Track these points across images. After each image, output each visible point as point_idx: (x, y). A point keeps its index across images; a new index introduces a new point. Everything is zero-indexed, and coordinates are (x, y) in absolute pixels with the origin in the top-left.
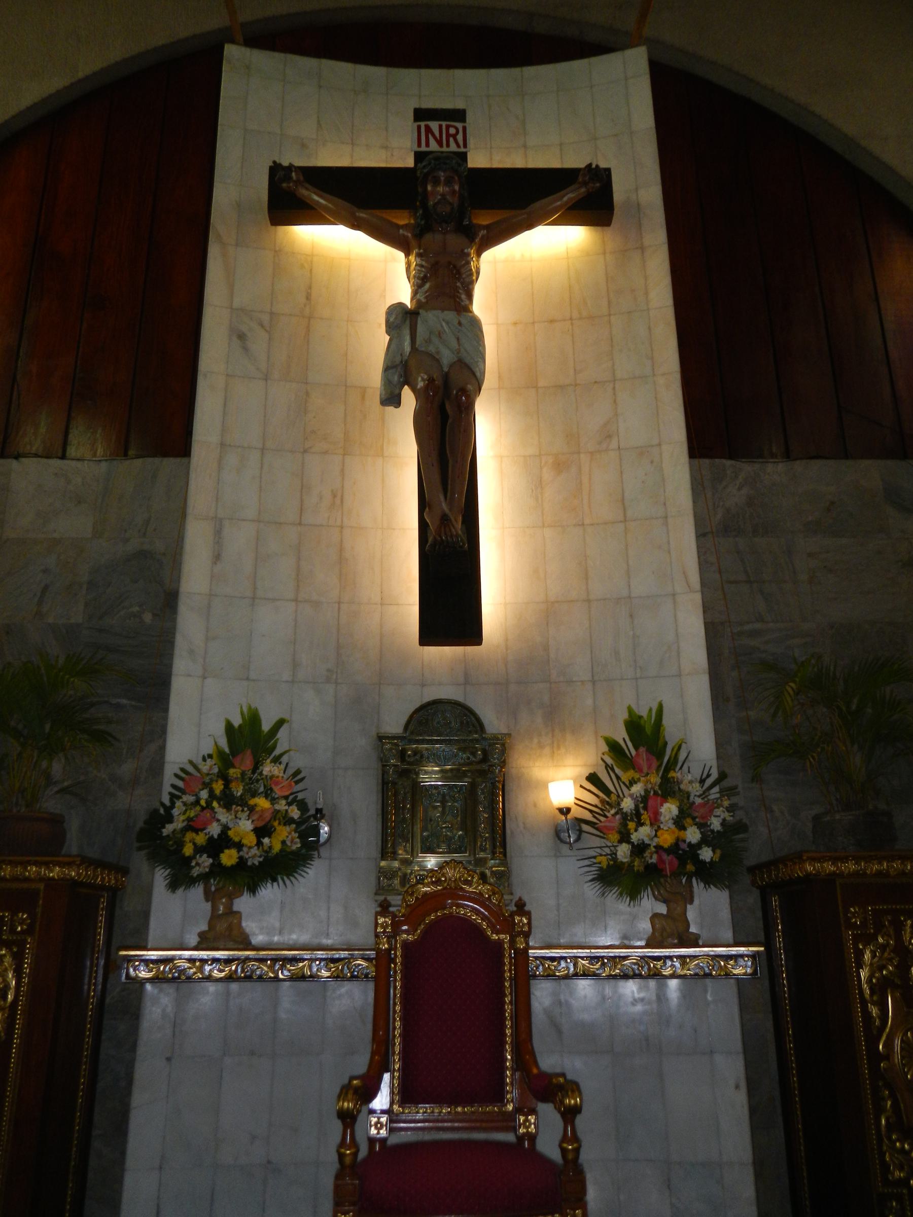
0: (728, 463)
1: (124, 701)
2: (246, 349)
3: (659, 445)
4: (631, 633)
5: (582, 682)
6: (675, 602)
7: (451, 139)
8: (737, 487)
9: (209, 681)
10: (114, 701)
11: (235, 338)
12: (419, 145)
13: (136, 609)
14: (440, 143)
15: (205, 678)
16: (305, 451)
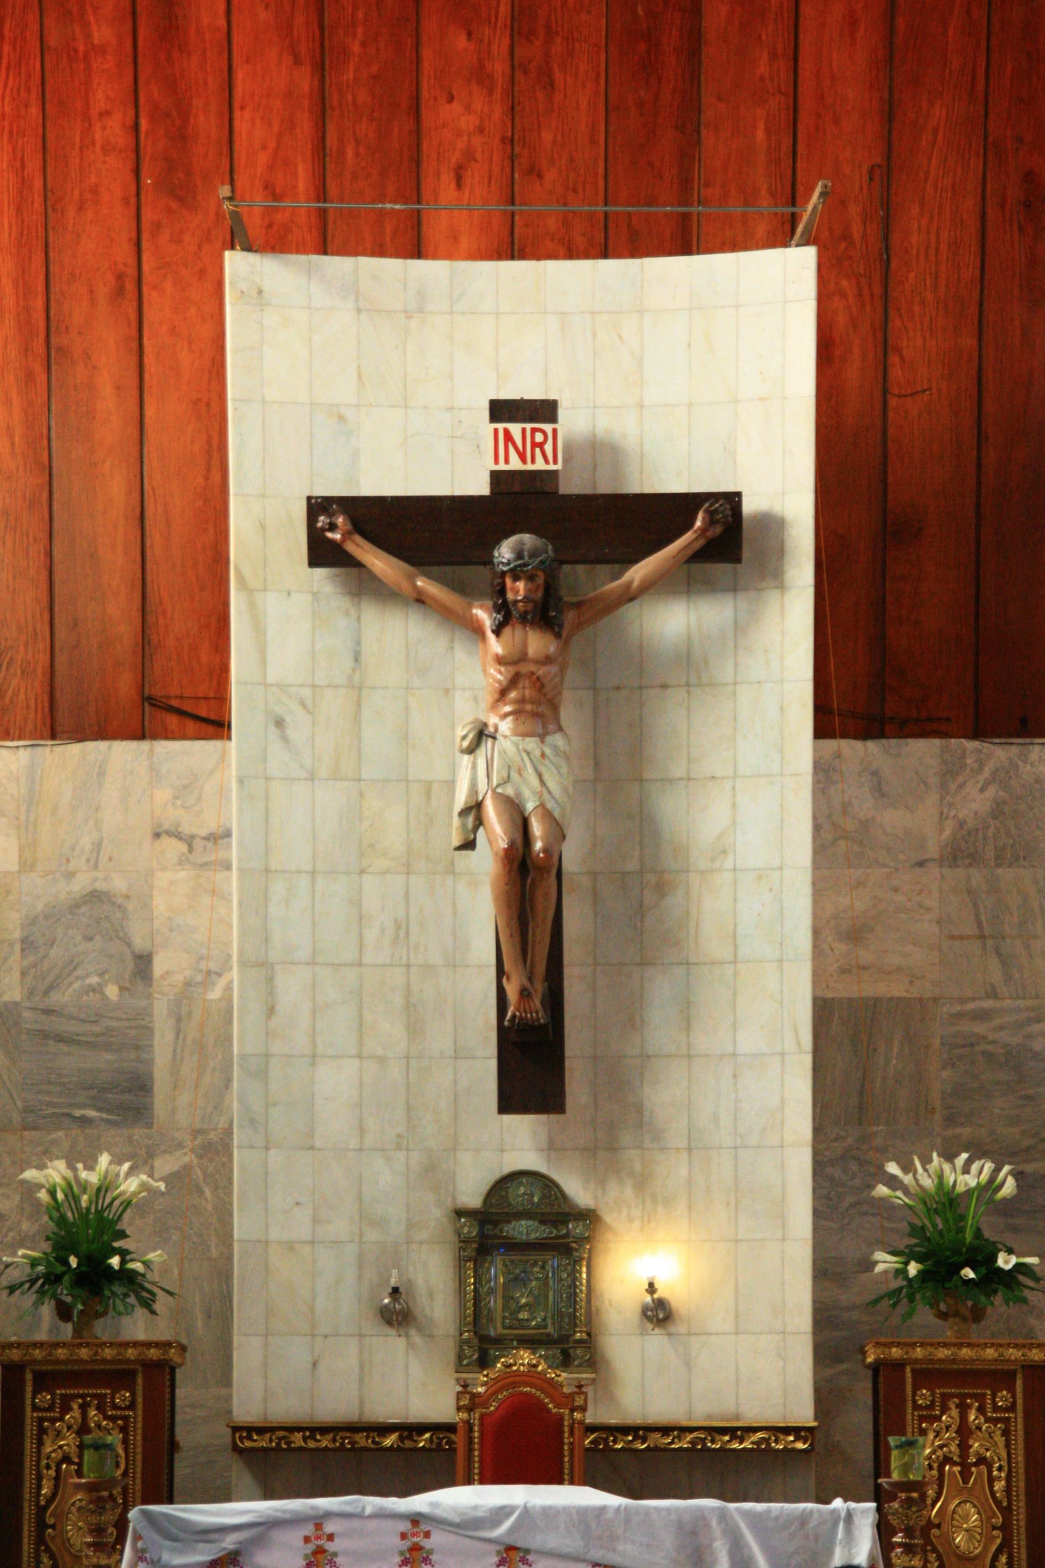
0: (971, 745)
1: (92, 1113)
2: (285, 739)
3: (781, 868)
4: (734, 1095)
5: (678, 1149)
6: (783, 1061)
7: (538, 450)
8: (979, 786)
9: (272, 1152)
10: (78, 1113)
11: (272, 728)
12: (496, 461)
13: (94, 980)
14: (523, 460)
15: (267, 1148)
16: (362, 872)
